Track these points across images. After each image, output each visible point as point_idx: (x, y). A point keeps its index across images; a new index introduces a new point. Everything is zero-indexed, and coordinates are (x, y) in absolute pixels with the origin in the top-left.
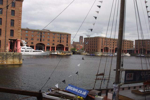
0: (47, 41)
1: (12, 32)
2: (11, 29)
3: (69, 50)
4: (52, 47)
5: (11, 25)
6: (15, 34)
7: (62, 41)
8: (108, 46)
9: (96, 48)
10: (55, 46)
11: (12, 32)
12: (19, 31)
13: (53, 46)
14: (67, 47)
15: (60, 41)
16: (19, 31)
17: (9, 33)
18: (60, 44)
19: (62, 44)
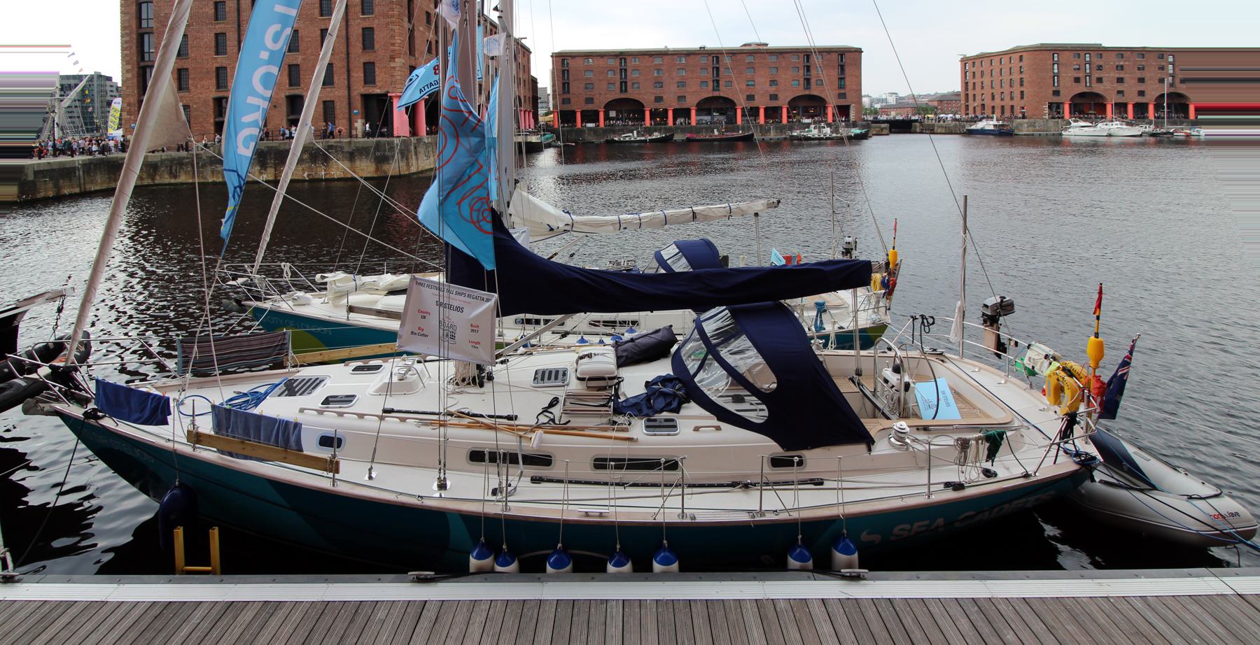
0: (744, 87)
1: (369, 69)
2: (363, 60)
3: (852, 116)
4: (766, 109)
5: (364, 48)
6: (380, 75)
7: (813, 81)
8: (1098, 88)
9: (1022, 97)
10: (783, 102)
11: (369, 69)
12: (393, 65)
13: (774, 104)
14: (843, 102)
15: (808, 81)
16: (393, 65)
17: (358, 75)
18: (807, 92)
19: (815, 91)
